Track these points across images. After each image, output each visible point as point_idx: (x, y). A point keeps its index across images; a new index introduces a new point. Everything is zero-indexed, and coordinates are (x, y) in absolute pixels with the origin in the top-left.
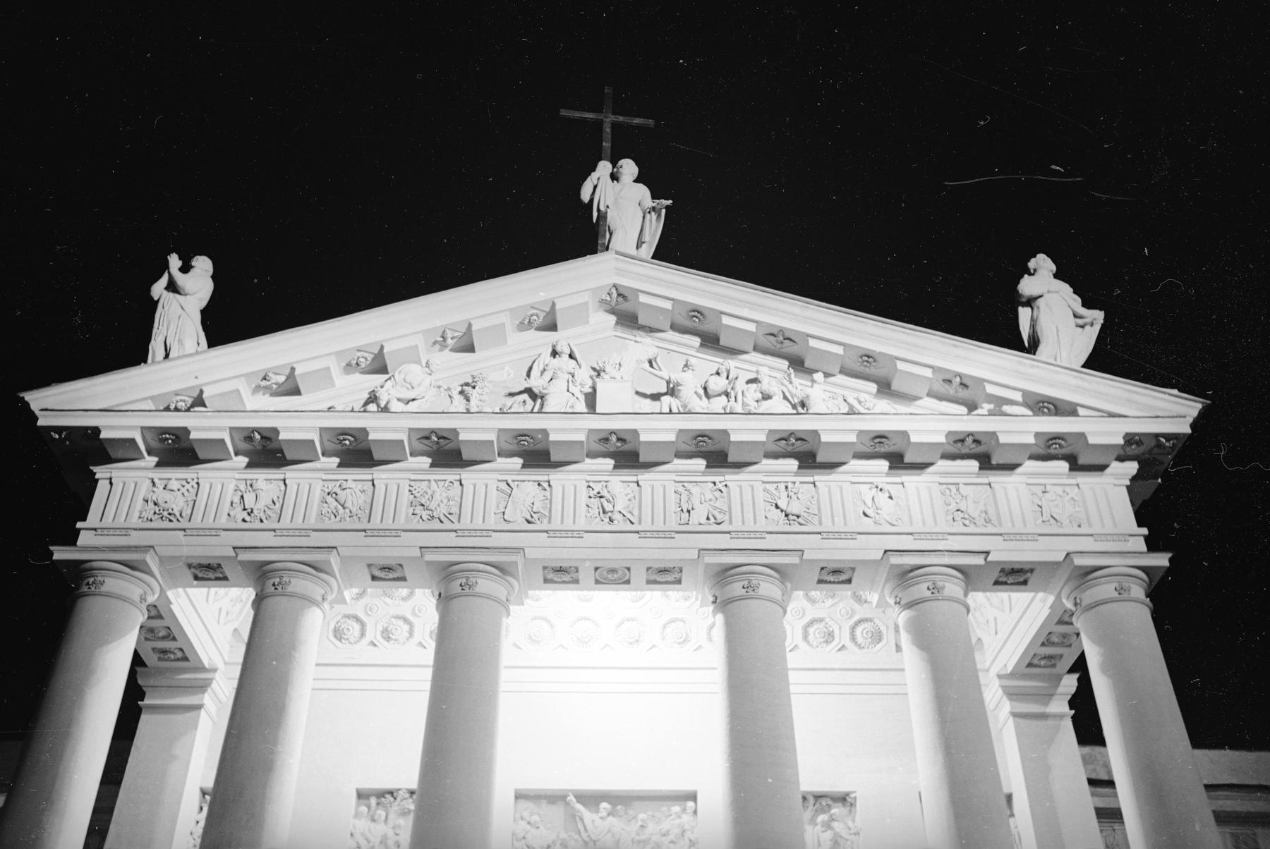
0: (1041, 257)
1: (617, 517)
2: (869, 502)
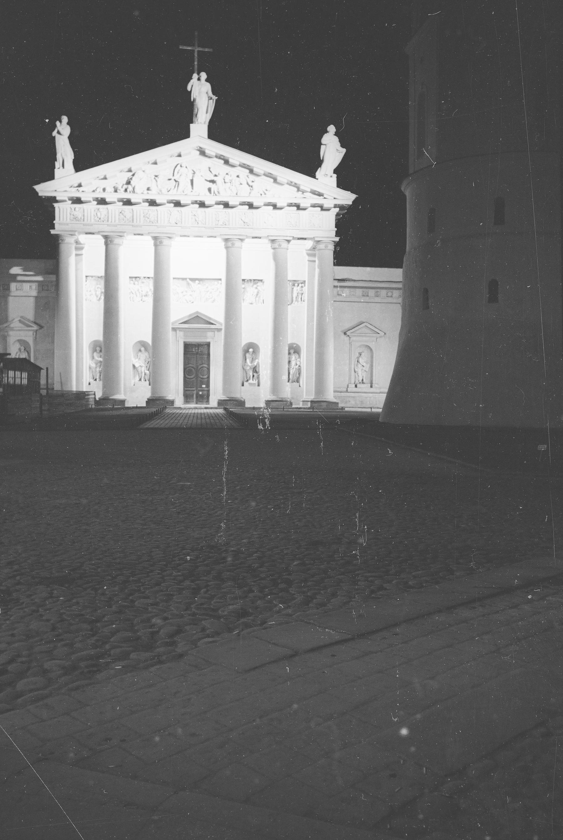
1: (199, 222)
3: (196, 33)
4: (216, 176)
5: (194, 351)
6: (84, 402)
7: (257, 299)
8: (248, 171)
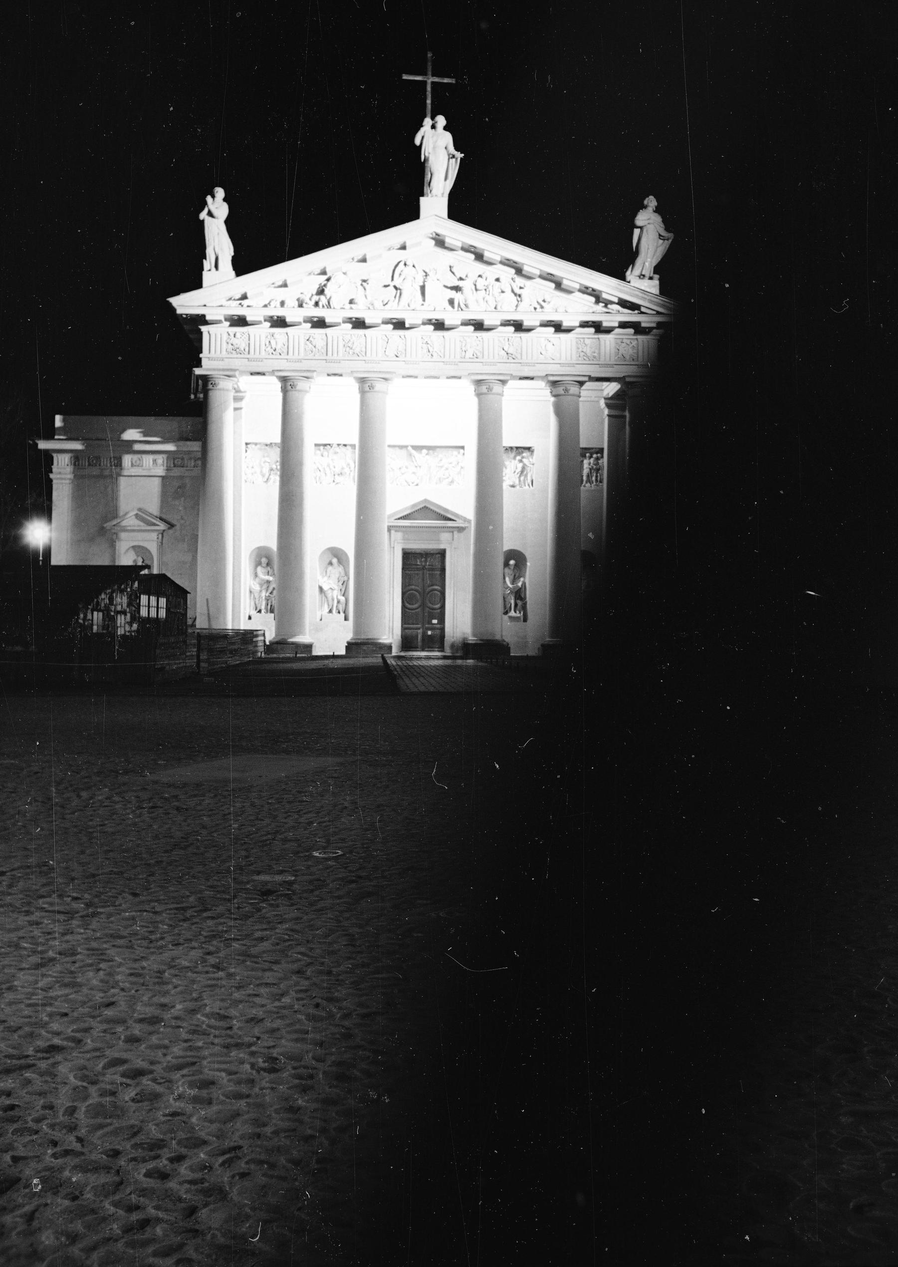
0: (651, 197)
1: (435, 354)
2: (543, 347)
3: (430, 55)
4: (461, 279)
5: (418, 563)
6: (251, 648)
7: (522, 478)
8: (513, 271)
